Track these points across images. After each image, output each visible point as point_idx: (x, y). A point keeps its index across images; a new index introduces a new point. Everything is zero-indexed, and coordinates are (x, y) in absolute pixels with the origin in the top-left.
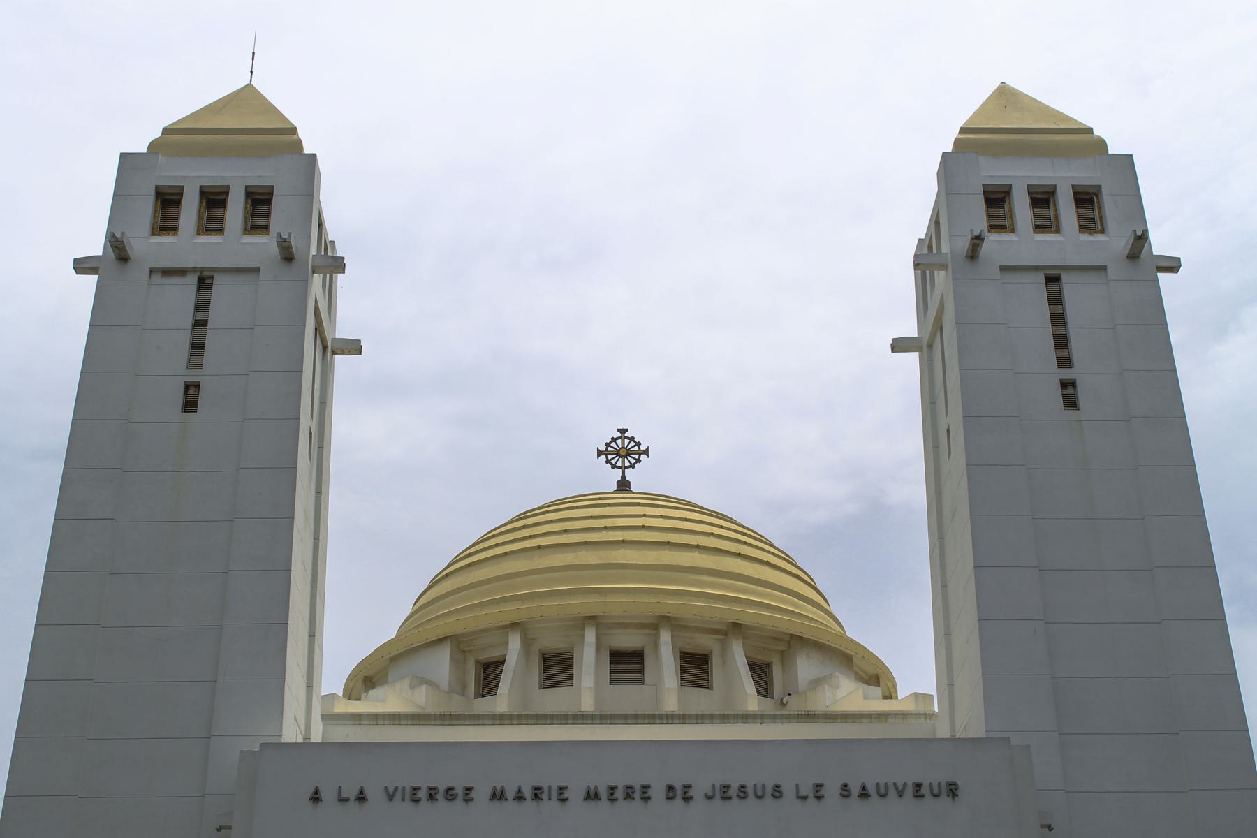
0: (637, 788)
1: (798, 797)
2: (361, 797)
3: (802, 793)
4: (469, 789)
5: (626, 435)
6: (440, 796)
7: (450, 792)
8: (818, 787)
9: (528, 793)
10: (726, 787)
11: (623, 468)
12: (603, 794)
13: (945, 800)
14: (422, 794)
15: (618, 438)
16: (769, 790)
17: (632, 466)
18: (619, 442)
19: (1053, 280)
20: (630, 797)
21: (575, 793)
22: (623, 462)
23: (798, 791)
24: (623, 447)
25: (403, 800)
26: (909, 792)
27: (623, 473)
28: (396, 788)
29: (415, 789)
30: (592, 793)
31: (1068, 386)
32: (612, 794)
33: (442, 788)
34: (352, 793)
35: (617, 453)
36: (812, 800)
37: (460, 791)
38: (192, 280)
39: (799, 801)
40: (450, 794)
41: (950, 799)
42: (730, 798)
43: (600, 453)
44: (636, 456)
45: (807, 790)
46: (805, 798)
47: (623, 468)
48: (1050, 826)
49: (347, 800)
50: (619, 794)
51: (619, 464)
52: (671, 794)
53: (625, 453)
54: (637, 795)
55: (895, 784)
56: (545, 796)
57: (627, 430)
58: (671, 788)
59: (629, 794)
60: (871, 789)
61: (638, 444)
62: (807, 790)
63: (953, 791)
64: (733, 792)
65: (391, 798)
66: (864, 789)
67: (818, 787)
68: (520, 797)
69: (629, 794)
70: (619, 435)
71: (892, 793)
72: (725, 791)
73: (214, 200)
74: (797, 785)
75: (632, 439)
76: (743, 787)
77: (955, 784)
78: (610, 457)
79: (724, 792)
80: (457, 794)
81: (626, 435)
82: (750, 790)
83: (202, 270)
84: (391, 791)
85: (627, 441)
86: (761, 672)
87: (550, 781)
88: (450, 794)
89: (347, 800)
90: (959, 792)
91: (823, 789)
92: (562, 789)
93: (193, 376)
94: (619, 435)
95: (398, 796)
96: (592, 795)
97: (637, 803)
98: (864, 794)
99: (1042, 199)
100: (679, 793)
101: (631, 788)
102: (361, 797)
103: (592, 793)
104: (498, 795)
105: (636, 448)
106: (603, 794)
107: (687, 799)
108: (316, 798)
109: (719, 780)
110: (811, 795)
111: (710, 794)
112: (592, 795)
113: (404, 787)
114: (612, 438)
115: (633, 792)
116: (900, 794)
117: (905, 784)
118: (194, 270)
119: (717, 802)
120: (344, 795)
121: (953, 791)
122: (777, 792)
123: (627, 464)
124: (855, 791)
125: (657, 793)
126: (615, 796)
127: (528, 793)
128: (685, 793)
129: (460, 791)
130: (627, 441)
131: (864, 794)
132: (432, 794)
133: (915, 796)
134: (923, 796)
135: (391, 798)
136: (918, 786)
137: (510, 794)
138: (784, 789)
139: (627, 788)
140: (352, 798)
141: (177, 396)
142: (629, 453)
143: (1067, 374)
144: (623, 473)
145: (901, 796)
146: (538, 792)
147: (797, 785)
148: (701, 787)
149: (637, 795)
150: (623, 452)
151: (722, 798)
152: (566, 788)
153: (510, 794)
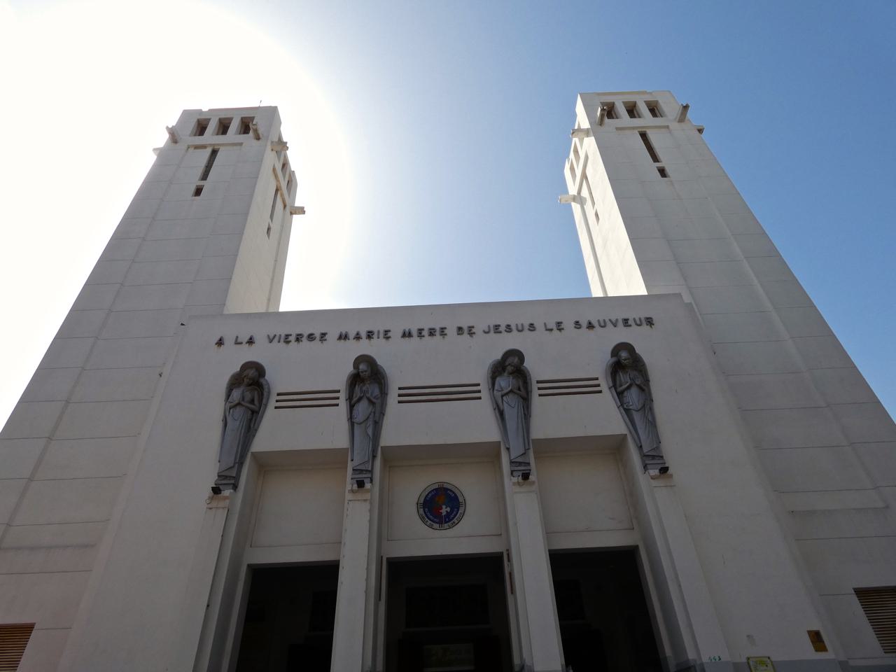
1: (547, 330)
3: (549, 327)
4: (324, 335)
6: (304, 339)
8: (559, 324)
9: (363, 335)
12: (415, 333)
13: (645, 328)
14: (292, 338)
16: (526, 327)
20: (433, 335)
21: (396, 333)
26: (620, 324)
28: (275, 336)
29: (287, 336)
30: (407, 334)
32: (420, 333)
33: (306, 335)
36: (556, 332)
37: (318, 336)
39: (548, 332)
40: (311, 337)
41: (649, 327)
42: (501, 332)
45: (552, 325)
46: (551, 330)
49: (241, 343)
50: (425, 333)
52: (460, 332)
54: (438, 333)
55: (610, 320)
56: (375, 336)
58: (460, 329)
59: (432, 333)
60: (595, 323)
62: (552, 325)
64: (502, 328)
65: (271, 341)
66: (590, 323)
67: (559, 324)
69: (432, 333)
74: (545, 324)
77: (651, 318)
82: (513, 327)
83: (214, 145)
84: (271, 337)
87: (378, 327)
88: (311, 337)
89: (241, 343)
90: (654, 322)
91: (562, 325)
92: (386, 332)
96: (407, 334)
97: (438, 337)
100: (466, 331)
101: (433, 329)
103: (407, 334)
106: (415, 333)
107: (471, 334)
108: (220, 343)
109: (493, 323)
110: (555, 328)
111: (486, 330)
112: (407, 334)
113: (280, 335)
115: (435, 332)
116: (615, 325)
117: (617, 320)
118: (211, 145)
121: (650, 322)
122: (532, 327)
124: (584, 324)
126: (423, 334)
127: (363, 335)
129: (318, 336)
133: (625, 326)
135: (271, 341)
137: (352, 335)
138: (536, 325)
139: (430, 329)
141: (193, 189)
145: (615, 326)
146: (370, 334)
147: (545, 324)
149: (438, 333)
151: (495, 332)
152: (390, 331)
153: (352, 335)
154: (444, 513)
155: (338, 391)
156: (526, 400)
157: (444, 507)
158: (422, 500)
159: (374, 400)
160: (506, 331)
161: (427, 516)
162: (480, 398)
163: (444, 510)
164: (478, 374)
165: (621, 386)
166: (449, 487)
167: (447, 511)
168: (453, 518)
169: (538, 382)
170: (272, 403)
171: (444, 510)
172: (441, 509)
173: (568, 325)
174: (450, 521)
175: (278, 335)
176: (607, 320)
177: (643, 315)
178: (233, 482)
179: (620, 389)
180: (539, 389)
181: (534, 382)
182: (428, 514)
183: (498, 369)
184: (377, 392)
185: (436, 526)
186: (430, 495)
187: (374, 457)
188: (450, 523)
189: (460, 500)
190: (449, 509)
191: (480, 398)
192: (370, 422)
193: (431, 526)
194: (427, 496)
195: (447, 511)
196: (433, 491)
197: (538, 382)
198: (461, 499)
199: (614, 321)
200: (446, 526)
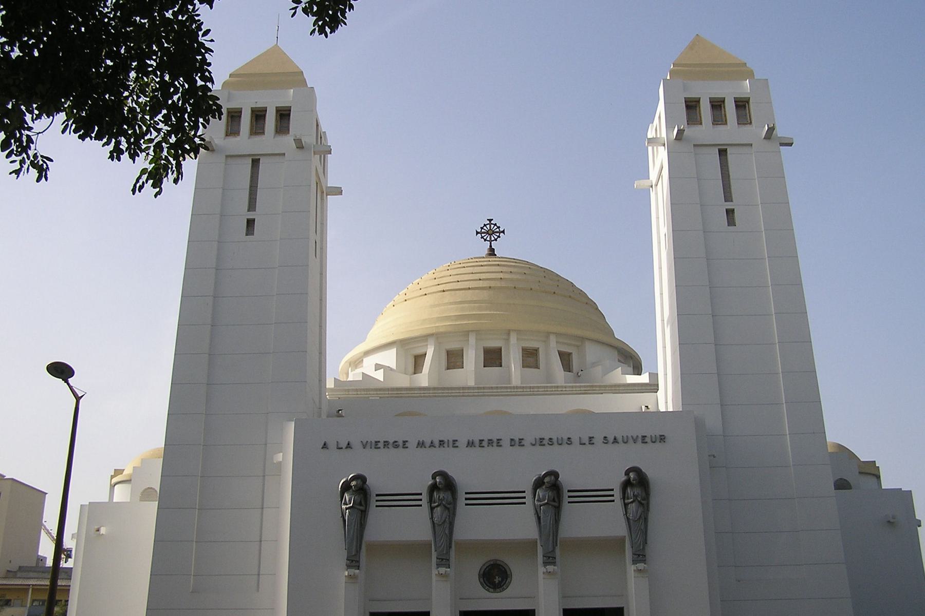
0: (495, 440)
2: (349, 446)
5: (492, 222)
7: (396, 444)
8: (591, 438)
9: (437, 443)
10: (542, 439)
11: (491, 241)
13: (658, 445)
14: (381, 445)
15: (487, 224)
17: (496, 240)
18: (488, 226)
19: (723, 153)
22: (490, 238)
23: (580, 441)
24: (490, 229)
25: (371, 448)
27: (491, 243)
28: (367, 442)
31: (730, 213)
33: (391, 441)
34: (344, 445)
35: (487, 233)
38: (249, 161)
40: (395, 445)
42: (544, 445)
43: (477, 233)
44: (498, 234)
47: (491, 241)
48: (714, 455)
49: (342, 448)
51: (488, 239)
53: (491, 233)
54: (495, 444)
55: (632, 436)
56: (446, 445)
57: (492, 220)
60: (620, 439)
61: (499, 227)
63: (662, 438)
67: (591, 438)
68: (432, 445)
69: (490, 442)
70: (488, 222)
71: (631, 441)
72: (541, 442)
73: (259, 115)
75: (495, 225)
76: (550, 439)
78: (483, 235)
79: (541, 442)
80: (399, 445)
81: (492, 222)
82: (555, 440)
84: (365, 442)
85: (492, 226)
86: (566, 359)
87: (447, 436)
88: (395, 445)
93: (251, 215)
94: (488, 222)
95: (369, 445)
96: (470, 444)
98: (615, 440)
99: (717, 105)
102: (349, 446)
104: (421, 444)
105: (498, 230)
106: (477, 443)
108: (325, 446)
110: (587, 443)
111: (534, 443)
112: (470, 444)
114: (484, 224)
119: (538, 448)
120: (340, 446)
123: (493, 239)
124: (611, 439)
125: (506, 443)
128: (520, 442)
129: (401, 444)
130: (492, 226)
131: (615, 440)
132: (386, 444)
134: (646, 442)
136: (644, 437)
137: (428, 443)
140: (344, 448)
142: (494, 232)
143: (729, 205)
144: (491, 243)
148: (529, 439)
149: (495, 444)
150: (490, 232)
151: (540, 445)
154: (497, 582)
155: (421, 494)
156: (558, 509)
157: (497, 577)
158: (482, 572)
159: (448, 506)
160: (548, 444)
161: (485, 583)
162: (524, 503)
163: (497, 580)
164: (526, 484)
165: (628, 499)
166: (502, 564)
167: (499, 581)
168: (503, 585)
169: (569, 491)
170: (373, 503)
171: (497, 580)
172: (496, 578)
173: (598, 439)
174: (501, 587)
175: (369, 441)
176: (630, 436)
177: (658, 433)
178: (357, 564)
179: (626, 501)
180: (569, 497)
181: (565, 491)
182: (487, 582)
183: (539, 483)
184: (450, 499)
185: (491, 590)
186: (487, 569)
187: (450, 547)
188: (501, 589)
189: (508, 573)
190: (500, 579)
191: (524, 503)
192: (447, 525)
193: (488, 591)
194: (486, 569)
195: (499, 581)
196: (489, 565)
197: (569, 491)
198: (509, 573)
199: (635, 437)
200: (498, 590)
